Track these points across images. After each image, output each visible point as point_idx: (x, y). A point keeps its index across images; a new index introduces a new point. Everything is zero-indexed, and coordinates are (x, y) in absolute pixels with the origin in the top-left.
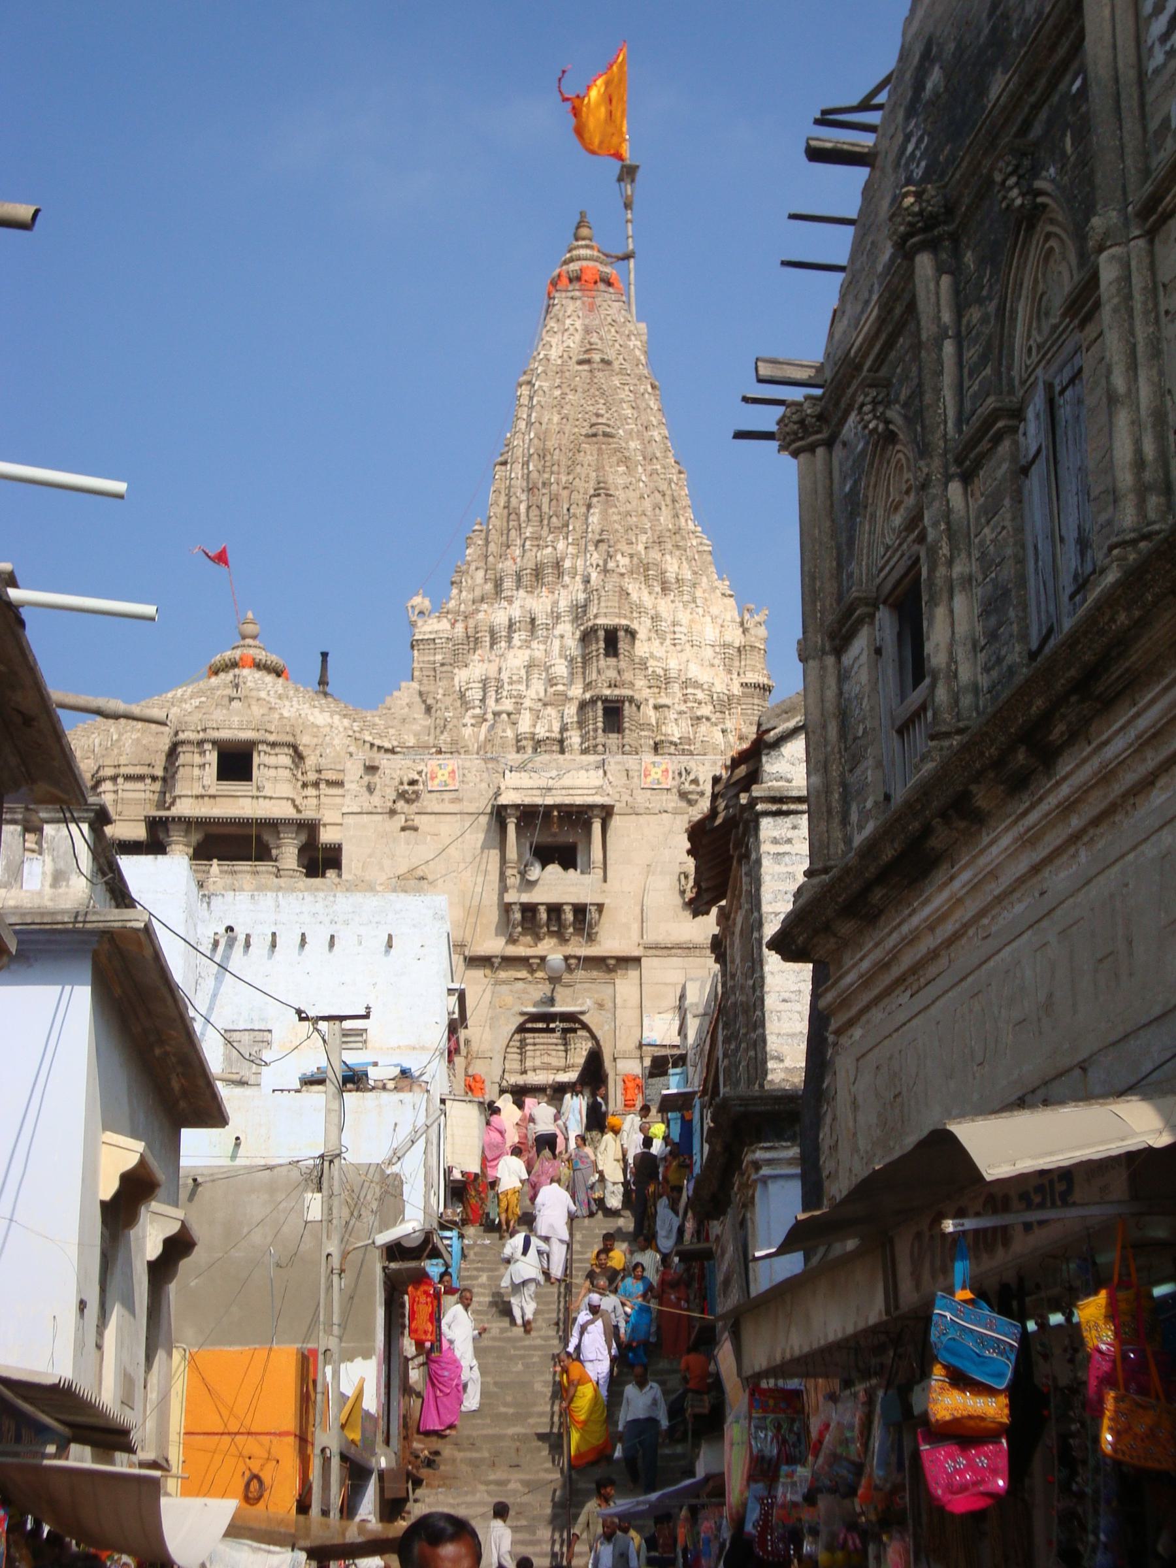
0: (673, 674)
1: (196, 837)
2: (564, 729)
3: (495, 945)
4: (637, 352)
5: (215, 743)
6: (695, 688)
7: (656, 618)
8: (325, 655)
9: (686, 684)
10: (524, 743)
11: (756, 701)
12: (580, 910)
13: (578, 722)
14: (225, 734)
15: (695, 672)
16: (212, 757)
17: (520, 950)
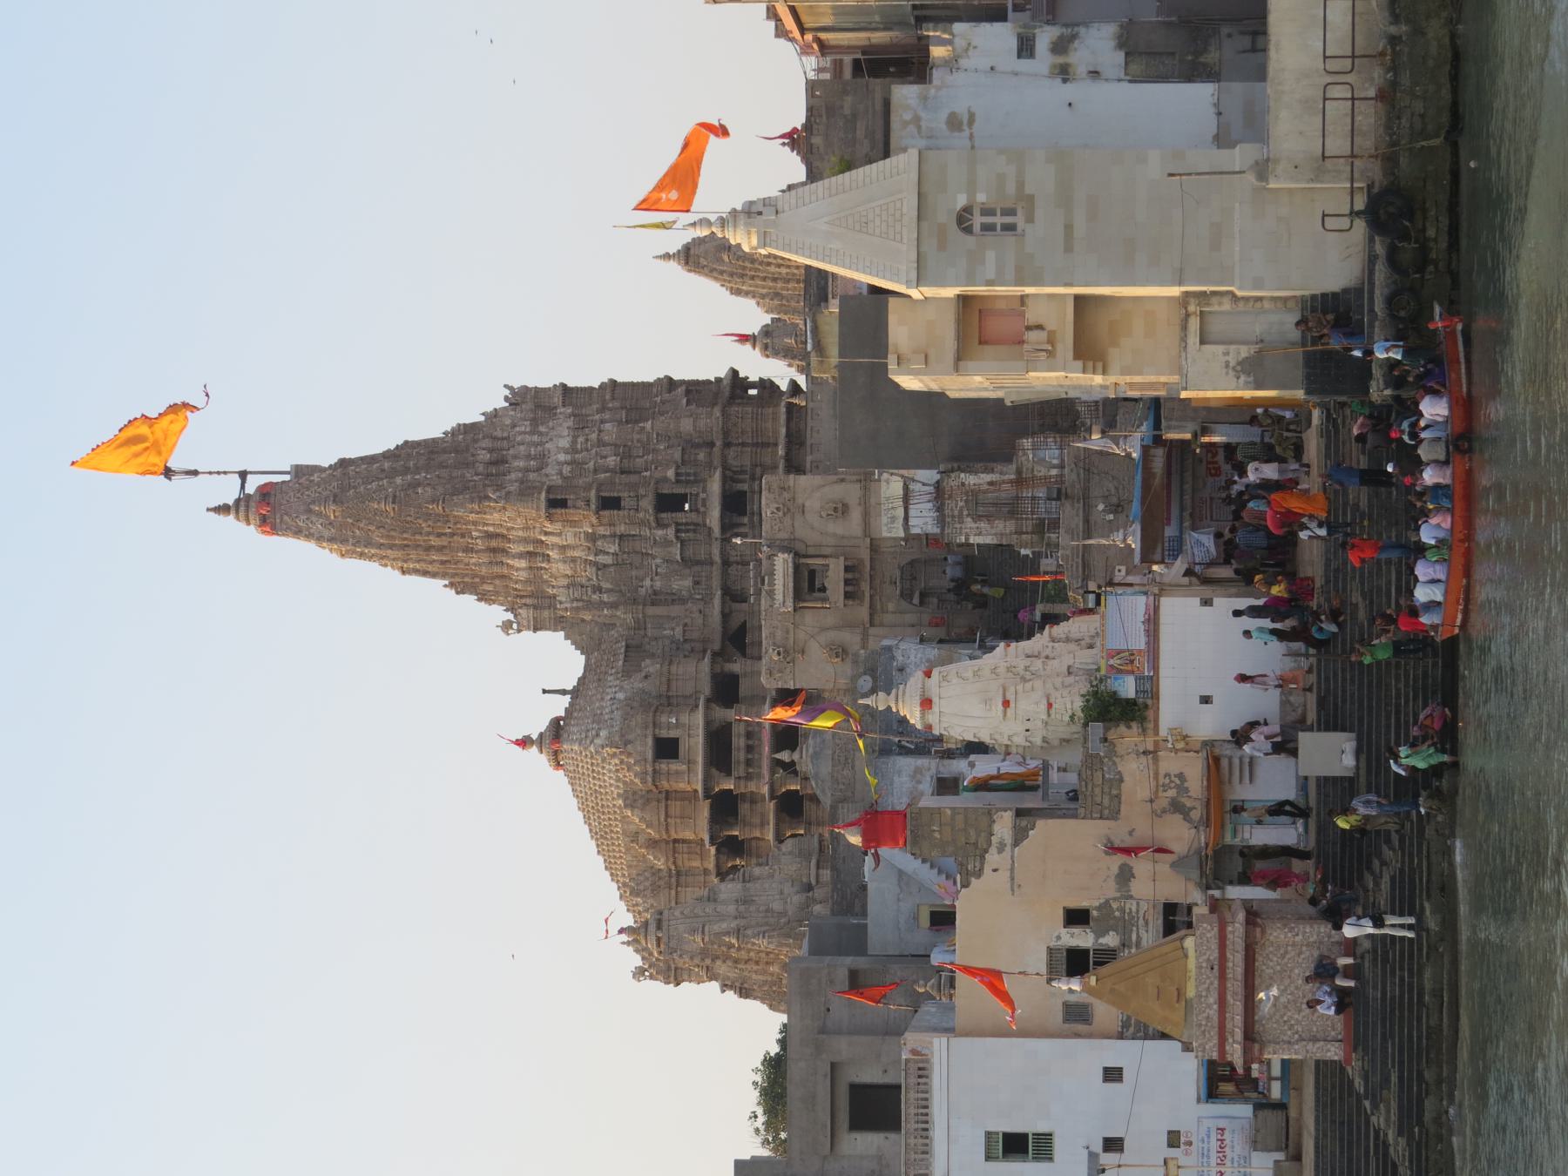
0: (569, 457)
1: (714, 770)
3: (863, 612)
7: (527, 470)
8: (544, 691)
9: (573, 450)
12: (847, 569)
14: (650, 755)
15: (565, 443)
16: (663, 766)
17: (867, 599)
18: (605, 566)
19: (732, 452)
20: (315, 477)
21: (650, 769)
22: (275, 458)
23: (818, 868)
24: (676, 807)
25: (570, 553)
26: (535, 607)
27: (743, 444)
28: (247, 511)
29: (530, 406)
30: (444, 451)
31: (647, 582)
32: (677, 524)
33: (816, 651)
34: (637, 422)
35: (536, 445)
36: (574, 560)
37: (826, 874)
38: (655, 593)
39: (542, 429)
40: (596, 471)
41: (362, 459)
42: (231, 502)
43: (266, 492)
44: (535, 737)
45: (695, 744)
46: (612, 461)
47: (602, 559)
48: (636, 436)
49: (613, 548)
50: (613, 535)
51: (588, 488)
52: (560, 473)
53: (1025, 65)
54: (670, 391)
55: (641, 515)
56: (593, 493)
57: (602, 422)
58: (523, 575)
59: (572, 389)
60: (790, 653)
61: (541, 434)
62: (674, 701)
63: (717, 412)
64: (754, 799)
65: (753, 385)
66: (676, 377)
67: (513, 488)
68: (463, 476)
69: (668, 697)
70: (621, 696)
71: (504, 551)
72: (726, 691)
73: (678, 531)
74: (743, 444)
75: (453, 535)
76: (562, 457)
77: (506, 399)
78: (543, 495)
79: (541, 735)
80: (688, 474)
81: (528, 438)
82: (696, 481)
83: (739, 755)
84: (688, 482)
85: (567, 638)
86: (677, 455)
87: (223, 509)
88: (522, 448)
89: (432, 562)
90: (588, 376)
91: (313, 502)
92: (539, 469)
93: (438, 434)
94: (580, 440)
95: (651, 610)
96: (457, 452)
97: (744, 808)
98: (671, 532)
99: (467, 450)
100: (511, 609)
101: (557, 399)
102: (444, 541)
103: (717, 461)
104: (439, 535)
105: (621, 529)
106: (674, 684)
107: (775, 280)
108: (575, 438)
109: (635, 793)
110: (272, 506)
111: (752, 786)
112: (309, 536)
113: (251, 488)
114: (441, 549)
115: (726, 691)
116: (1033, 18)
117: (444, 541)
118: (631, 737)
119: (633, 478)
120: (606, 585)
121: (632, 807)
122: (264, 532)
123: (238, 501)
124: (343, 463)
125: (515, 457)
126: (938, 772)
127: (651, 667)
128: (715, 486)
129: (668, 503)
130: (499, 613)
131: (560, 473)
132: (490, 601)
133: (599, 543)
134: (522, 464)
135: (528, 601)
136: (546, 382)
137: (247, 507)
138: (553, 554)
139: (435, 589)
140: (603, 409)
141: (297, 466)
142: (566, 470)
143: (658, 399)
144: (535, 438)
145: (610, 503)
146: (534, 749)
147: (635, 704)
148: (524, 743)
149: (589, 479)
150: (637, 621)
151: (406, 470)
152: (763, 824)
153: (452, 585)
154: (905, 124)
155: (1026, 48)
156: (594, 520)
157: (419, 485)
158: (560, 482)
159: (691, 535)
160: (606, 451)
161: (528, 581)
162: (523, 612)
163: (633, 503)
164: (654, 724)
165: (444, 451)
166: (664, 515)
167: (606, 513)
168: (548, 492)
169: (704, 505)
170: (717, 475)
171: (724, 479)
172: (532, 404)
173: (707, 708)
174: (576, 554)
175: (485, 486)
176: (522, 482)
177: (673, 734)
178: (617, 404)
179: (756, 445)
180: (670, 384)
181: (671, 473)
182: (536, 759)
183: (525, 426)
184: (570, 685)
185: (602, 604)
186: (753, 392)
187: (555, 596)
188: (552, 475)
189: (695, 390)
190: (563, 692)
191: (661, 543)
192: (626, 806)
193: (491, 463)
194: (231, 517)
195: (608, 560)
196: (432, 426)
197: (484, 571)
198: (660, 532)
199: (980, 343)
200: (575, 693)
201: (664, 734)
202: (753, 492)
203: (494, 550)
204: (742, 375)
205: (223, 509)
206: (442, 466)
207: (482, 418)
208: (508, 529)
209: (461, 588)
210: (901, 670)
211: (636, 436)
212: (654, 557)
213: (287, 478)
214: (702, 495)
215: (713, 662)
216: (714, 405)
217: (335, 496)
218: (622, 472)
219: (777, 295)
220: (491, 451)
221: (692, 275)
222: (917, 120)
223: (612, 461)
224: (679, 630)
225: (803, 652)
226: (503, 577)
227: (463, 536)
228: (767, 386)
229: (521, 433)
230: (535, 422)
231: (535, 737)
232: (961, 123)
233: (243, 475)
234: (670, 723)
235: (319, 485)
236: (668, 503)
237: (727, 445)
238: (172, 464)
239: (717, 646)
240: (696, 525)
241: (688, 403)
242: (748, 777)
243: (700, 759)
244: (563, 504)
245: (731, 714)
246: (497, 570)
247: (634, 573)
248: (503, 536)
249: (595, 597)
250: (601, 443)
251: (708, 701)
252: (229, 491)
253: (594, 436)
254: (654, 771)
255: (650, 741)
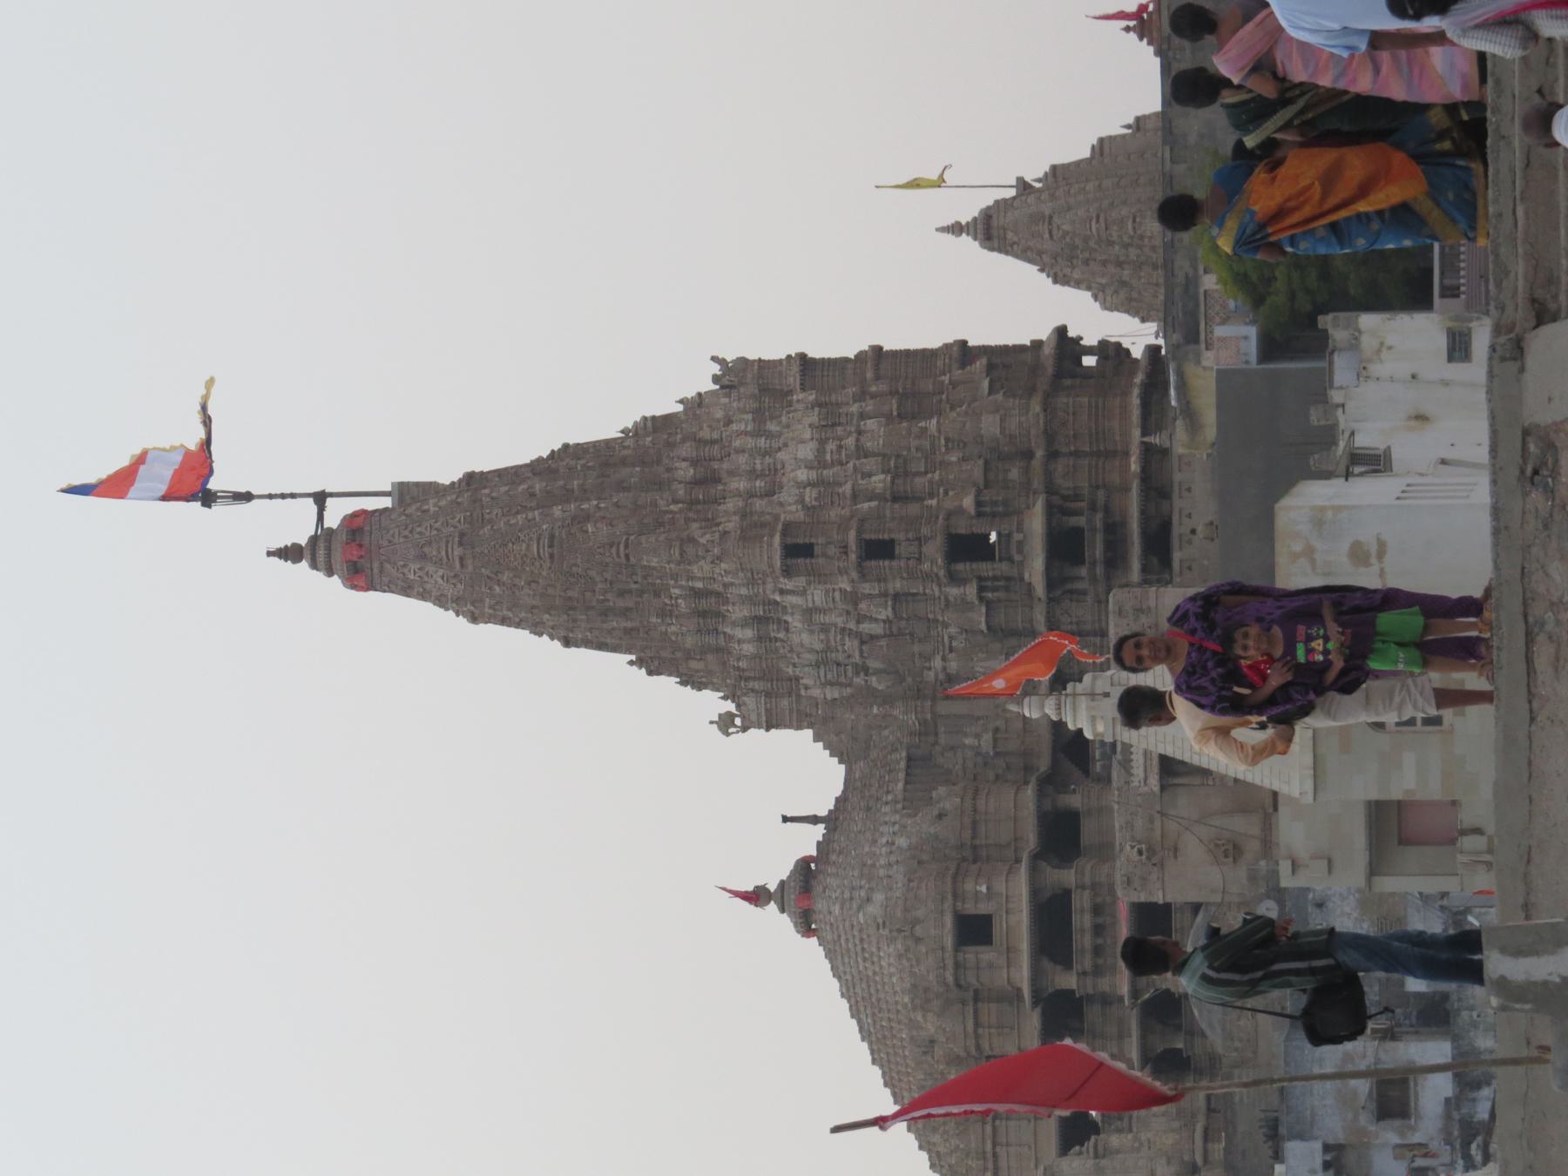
0: (813, 475)
1: (1047, 964)
2: (884, 595)
4: (443, 503)
5: (956, 950)
6: (824, 452)
7: (751, 495)
8: (785, 819)
9: (819, 463)
10: (895, 630)
11: (818, 373)
13: (879, 581)
14: (949, 941)
15: (807, 451)
16: (971, 954)
18: (873, 637)
19: (1060, 466)
20: (431, 506)
21: (950, 963)
22: (368, 472)
23: (1206, 1139)
24: (990, 1011)
25: (822, 618)
26: (768, 695)
27: (1076, 454)
28: (329, 555)
29: (752, 389)
30: (624, 462)
31: (937, 663)
32: (980, 579)
33: (1193, 849)
34: (914, 417)
35: (766, 453)
36: (825, 629)
37: (1218, 1149)
38: (951, 679)
39: (772, 427)
40: (855, 497)
41: (499, 473)
42: (303, 542)
43: (357, 524)
44: (772, 887)
45: (1017, 923)
46: (879, 481)
47: (866, 627)
48: (914, 443)
49: (886, 613)
50: (884, 595)
51: (843, 526)
52: (801, 501)
53: (1458, 371)
54: (963, 365)
55: (926, 566)
56: (852, 535)
57: (863, 416)
58: (749, 649)
59: (814, 360)
60: (1157, 853)
61: (769, 435)
62: (984, 853)
63: (1036, 407)
64: (1107, 1000)
65: (1089, 351)
66: (973, 342)
67: (732, 524)
68: (654, 504)
69: (974, 847)
70: (902, 842)
71: (718, 614)
72: (1062, 836)
73: (981, 589)
74: (1076, 454)
75: (641, 593)
76: (803, 475)
77: (716, 379)
78: (777, 539)
79: (782, 883)
80: (995, 503)
81: (750, 442)
82: (1006, 514)
83: (1083, 940)
84: (994, 515)
85: (816, 739)
86: (977, 472)
87: (290, 553)
88: (742, 459)
89: (610, 632)
90: (837, 341)
91: (430, 543)
92: (770, 493)
93: (613, 432)
94: (831, 446)
95: (944, 708)
96: (643, 463)
97: (1093, 1013)
98: (971, 591)
99: (659, 462)
100: (730, 696)
101: (793, 378)
102: (629, 602)
103: (1037, 483)
104: (622, 593)
105: (897, 585)
106: (982, 828)
107: (1120, 264)
108: (822, 442)
109: (926, 990)
110: (363, 549)
111: (1104, 984)
112: (423, 596)
113: (333, 519)
114: (625, 613)
115: (1062, 836)
116: (1469, 306)
117: (629, 602)
118: (920, 913)
119: (913, 509)
120: (874, 664)
121: (925, 1010)
122: (354, 587)
123: (314, 540)
124: (470, 478)
125: (731, 473)
126: (1378, 1061)
127: (946, 798)
128: (1036, 522)
129: (966, 548)
130: (713, 703)
131: (801, 501)
132: (699, 686)
133: (863, 606)
134: (741, 484)
135: (756, 685)
136: (774, 348)
137: (329, 549)
138: (795, 622)
139: (617, 664)
140: (862, 396)
141: (401, 484)
142: (810, 495)
143: (946, 379)
144: (762, 442)
145: (877, 550)
146: (772, 907)
147: (925, 857)
148: (757, 897)
149: (846, 512)
150: (923, 723)
151: (567, 496)
152: (1122, 1035)
153: (639, 663)
154: (1295, 557)
155: (1458, 348)
156: (854, 575)
157: (587, 518)
158: (801, 516)
159: (1001, 595)
160: (870, 464)
161: (754, 657)
162: (750, 701)
163: (914, 548)
164: (955, 896)
165: (624, 462)
166: (960, 567)
167: (873, 563)
168: (784, 534)
169: (1020, 551)
170: (1039, 508)
171: (1050, 509)
172: (753, 385)
173: (1034, 870)
174: (827, 619)
175: (687, 520)
176: (744, 516)
177: (983, 908)
178: (883, 387)
179: (1098, 454)
180: (963, 352)
181: (968, 502)
182: (776, 922)
183: (744, 423)
184: (824, 807)
185: (870, 694)
186: (1089, 361)
187: (797, 679)
188: (789, 506)
189: (1004, 364)
190: (814, 820)
191: (958, 603)
192: (914, 1009)
193: (697, 482)
194: (304, 564)
195: (877, 629)
196: (603, 419)
197: (689, 642)
198: (954, 591)
199: (1404, 841)
200: (831, 822)
201: (970, 908)
202: (1094, 530)
203: (703, 614)
204: (1071, 333)
205: (290, 553)
206: (621, 487)
207: (680, 408)
208: (725, 585)
209: (653, 664)
210: (1320, 905)
211: (914, 443)
212: (946, 625)
213: (386, 502)
214: (1017, 537)
215: (1041, 793)
216: (1031, 391)
217: (462, 535)
218: (895, 499)
219: (1123, 284)
220: (695, 463)
221: (995, 254)
222: (1309, 552)
223: (879, 481)
224: (987, 738)
225: (1176, 850)
226: (718, 650)
227: (657, 594)
228: (1112, 352)
229: (740, 434)
230: (759, 415)
231: (772, 887)
232: (1368, 555)
233: (320, 498)
234: (979, 893)
235: (436, 517)
236: (966, 548)
237: (1052, 455)
238: (213, 485)
239: (1044, 764)
240: (1008, 579)
241: (990, 394)
242: (1098, 971)
243: (1024, 946)
244: (806, 551)
245: (1067, 877)
246: (711, 640)
247: (916, 648)
248: (718, 594)
249: (859, 680)
250: (861, 452)
251: (1036, 857)
252: (299, 525)
253: (850, 441)
254: (957, 965)
255: (949, 921)
